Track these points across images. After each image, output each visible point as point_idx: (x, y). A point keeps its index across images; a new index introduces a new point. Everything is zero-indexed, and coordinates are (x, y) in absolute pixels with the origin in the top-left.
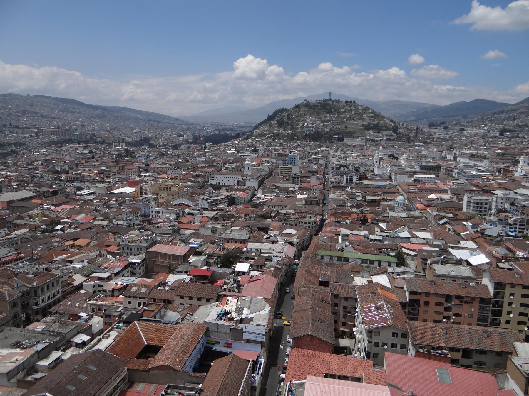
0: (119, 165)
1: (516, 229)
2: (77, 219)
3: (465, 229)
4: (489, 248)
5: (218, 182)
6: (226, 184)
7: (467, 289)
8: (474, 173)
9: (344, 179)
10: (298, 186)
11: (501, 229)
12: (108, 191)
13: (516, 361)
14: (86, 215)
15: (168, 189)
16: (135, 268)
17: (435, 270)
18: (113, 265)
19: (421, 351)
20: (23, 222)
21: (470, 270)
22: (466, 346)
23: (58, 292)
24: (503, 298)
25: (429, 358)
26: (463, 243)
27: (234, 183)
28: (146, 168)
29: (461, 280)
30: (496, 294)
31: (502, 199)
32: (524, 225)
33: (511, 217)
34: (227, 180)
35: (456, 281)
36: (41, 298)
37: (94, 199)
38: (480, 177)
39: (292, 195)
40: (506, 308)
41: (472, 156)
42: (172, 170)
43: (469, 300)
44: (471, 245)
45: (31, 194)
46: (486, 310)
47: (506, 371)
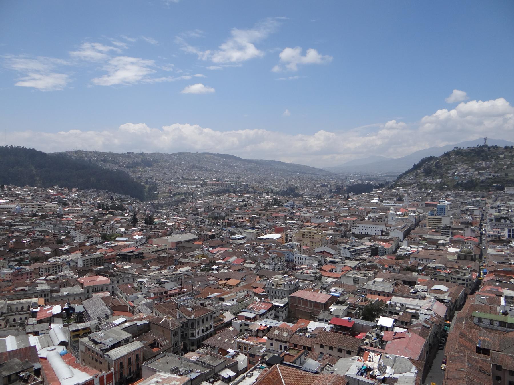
0: (268, 213)
2: (230, 260)
5: (361, 231)
6: (369, 234)
9: (506, 233)
10: (449, 238)
12: (257, 236)
14: (238, 257)
15: (311, 237)
16: (278, 312)
18: (258, 306)
20: (187, 260)
23: (211, 327)
27: (377, 232)
28: (291, 216)
34: (370, 229)
36: (197, 330)
37: (245, 243)
39: (442, 248)
42: (315, 219)
45: (195, 237)
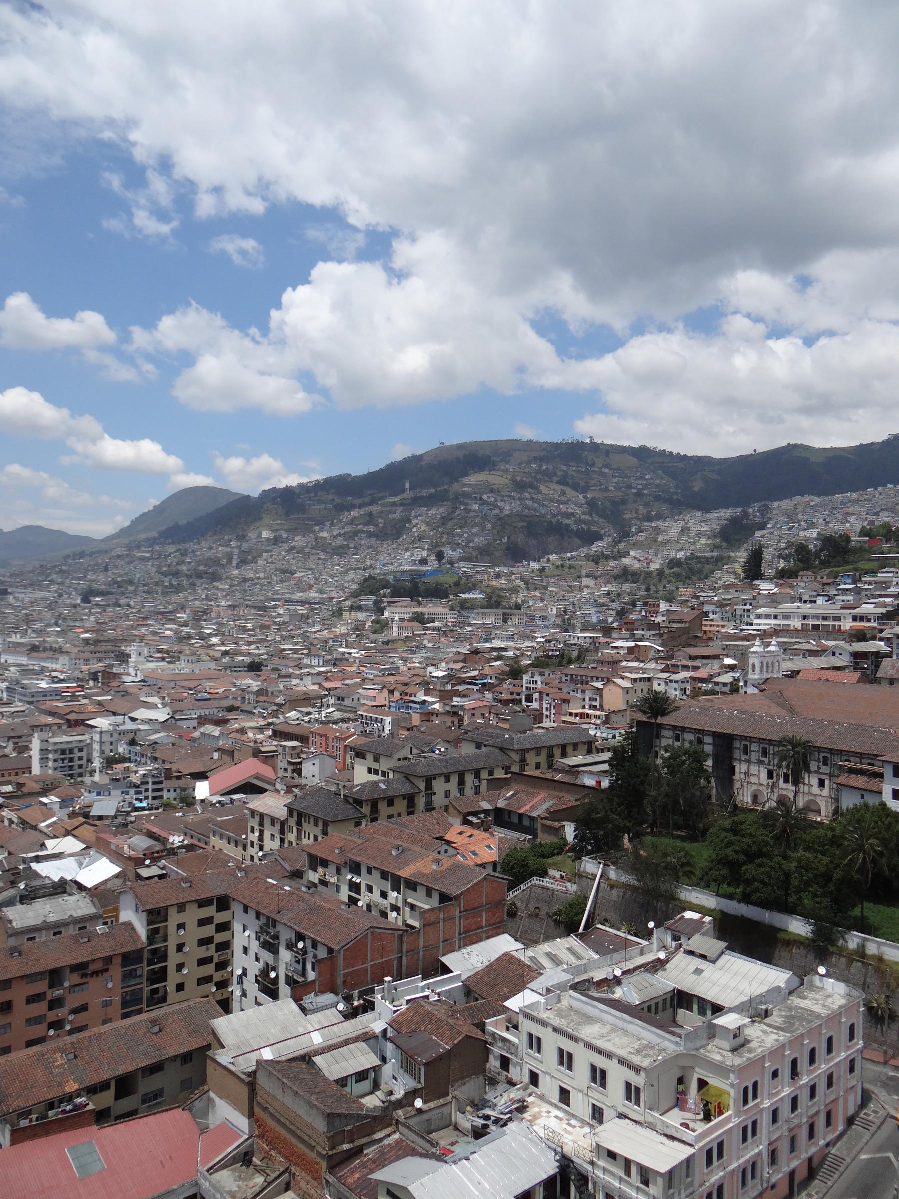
1: (147, 794)
3: (47, 811)
4: (116, 841)
7: (93, 943)
8: (44, 685)
11: (121, 799)
13: (223, 1057)
17: (11, 922)
19: (24, 1123)
21: (88, 900)
22: (122, 1070)
24: (166, 940)
25: (47, 1133)
26: (53, 846)
29: (71, 927)
30: (153, 934)
31: (112, 736)
32: (161, 782)
33: (135, 769)
35: (60, 933)
38: (58, 693)
40: (174, 958)
41: (34, 649)
43: (99, 966)
44: (71, 844)
46: (136, 977)
47: (206, 1088)
